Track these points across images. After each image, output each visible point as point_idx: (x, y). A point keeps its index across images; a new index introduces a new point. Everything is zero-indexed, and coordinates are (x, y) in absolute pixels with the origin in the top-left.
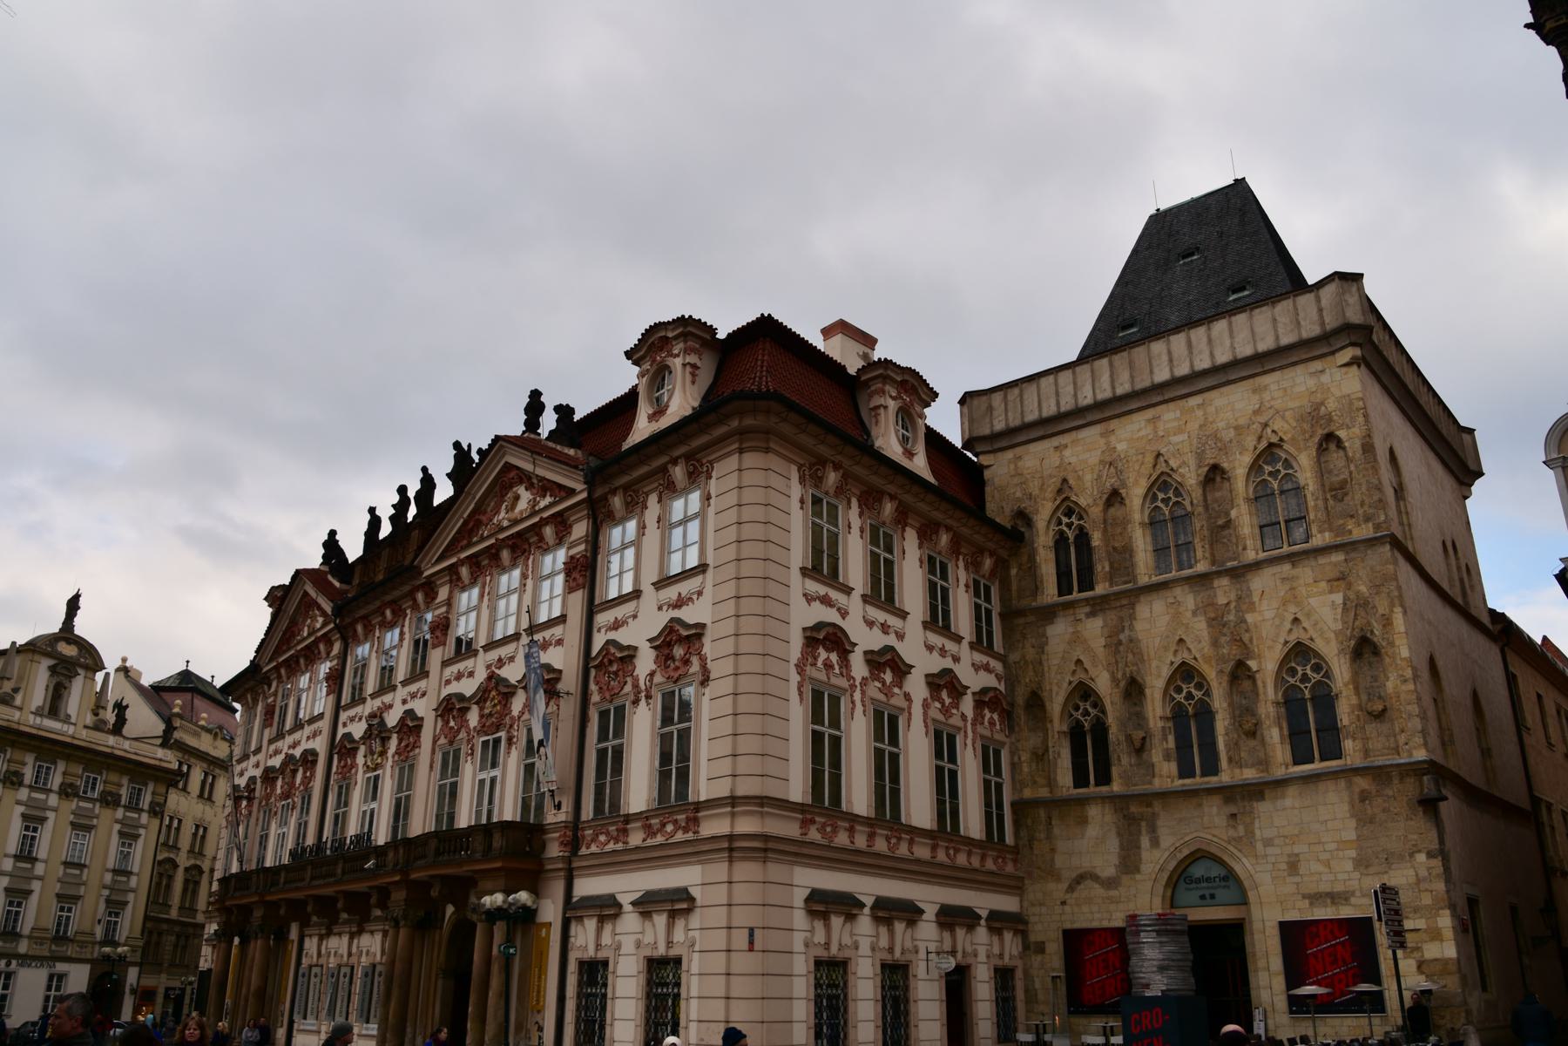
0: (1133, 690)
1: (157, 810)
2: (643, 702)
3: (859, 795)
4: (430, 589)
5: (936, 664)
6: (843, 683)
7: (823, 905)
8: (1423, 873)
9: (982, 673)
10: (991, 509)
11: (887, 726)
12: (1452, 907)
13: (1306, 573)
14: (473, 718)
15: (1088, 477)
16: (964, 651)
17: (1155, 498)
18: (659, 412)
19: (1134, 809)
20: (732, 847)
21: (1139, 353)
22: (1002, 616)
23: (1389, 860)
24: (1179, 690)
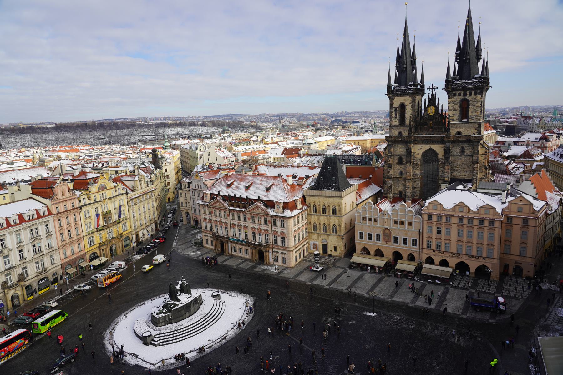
0: (320, 224)
7: (296, 252)
13: (335, 218)
23: (339, 242)
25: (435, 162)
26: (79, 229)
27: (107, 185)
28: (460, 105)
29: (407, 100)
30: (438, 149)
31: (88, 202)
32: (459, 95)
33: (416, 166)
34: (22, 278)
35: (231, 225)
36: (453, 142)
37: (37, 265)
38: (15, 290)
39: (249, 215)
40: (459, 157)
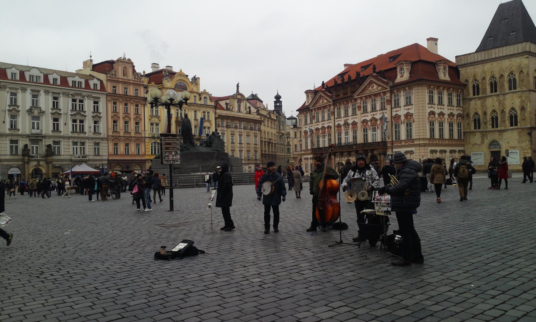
0: (485, 113)
1: (259, 130)
2: (403, 124)
3: (437, 136)
4: (356, 100)
5: (449, 112)
6: (434, 119)
7: (432, 152)
8: (527, 144)
9: (458, 111)
10: (461, 78)
11: (441, 124)
12: (532, 149)
13: (515, 95)
14: (369, 123)
15: (479, 74)
16: (455, 108)
17: (491, 79)
18: (402, 76)
19: (484, 133)
20: (419, 145)
22: (463, 99)
24: (493, 114)
26: (140, 124)
27: (189, 87)
34: (50, 151)
35: (336, 129)
37: (75, 147)
38: (38, 163)
39: (359, 101)
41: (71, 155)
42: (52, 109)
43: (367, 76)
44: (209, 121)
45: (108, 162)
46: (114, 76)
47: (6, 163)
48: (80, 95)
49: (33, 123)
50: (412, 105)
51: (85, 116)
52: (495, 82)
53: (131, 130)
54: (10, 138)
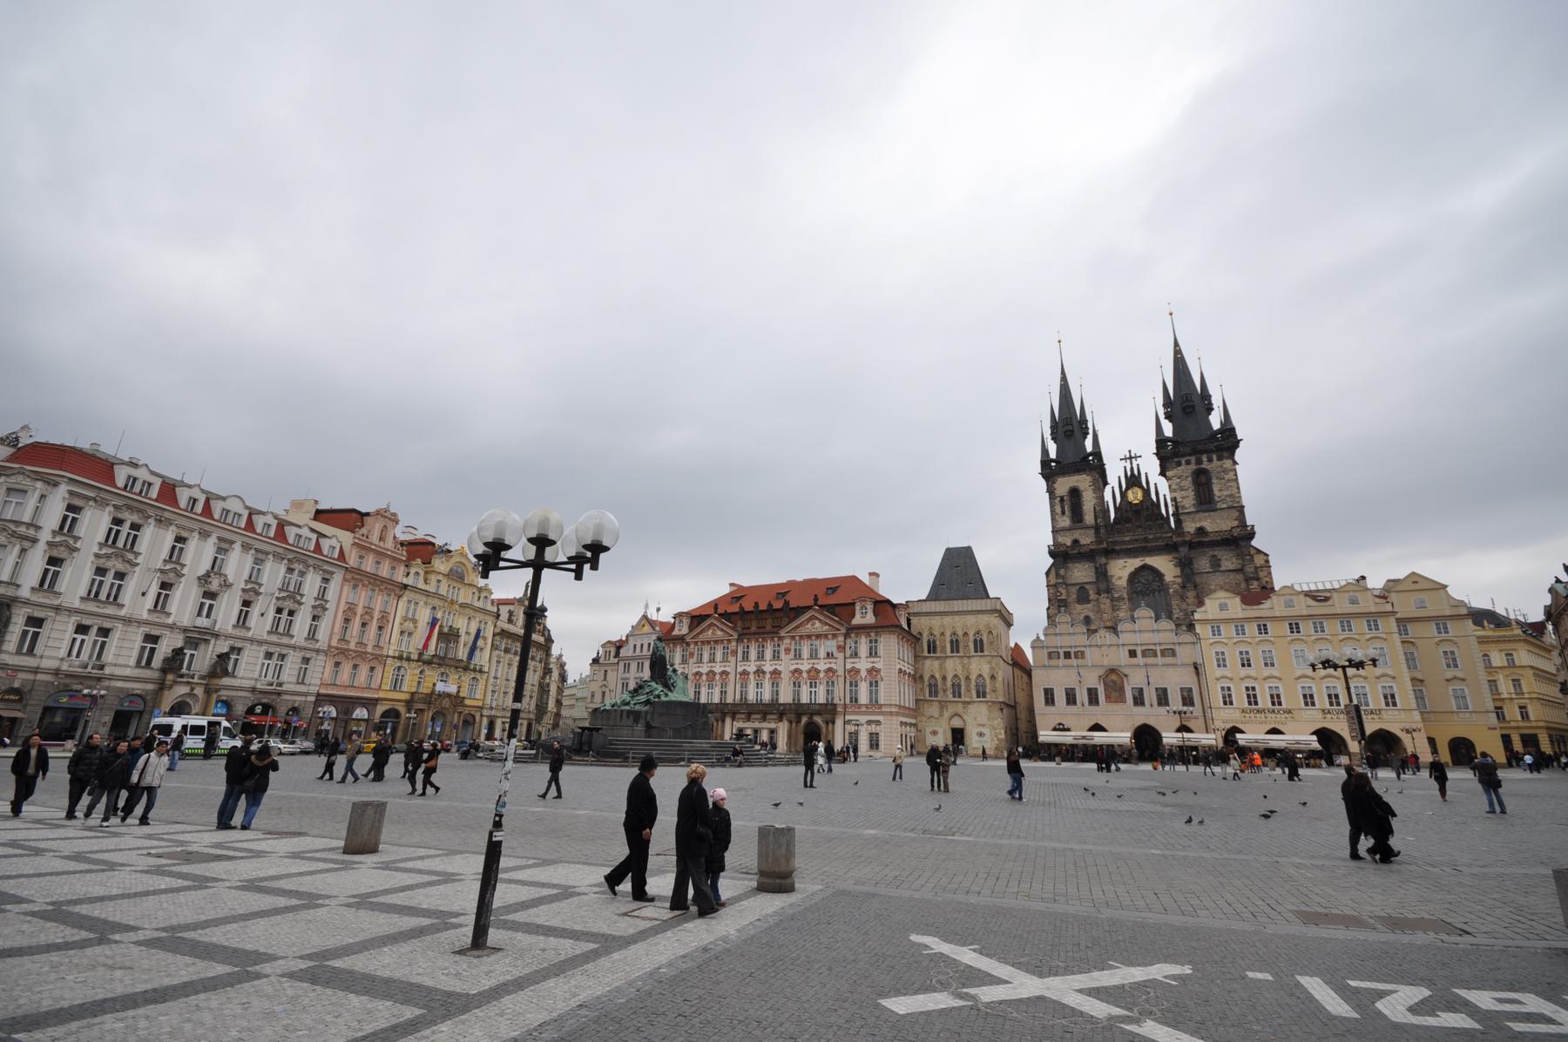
0: (944, 678)
4: (781, 638)
13: (982, 659)
14: (805, 675)
20: (891, 713)
21: (951, 602)
23: (994, 719)
25: (1159, 591)
26: (384, 630)
27: (468, 575)
28: (1193, 479)
29: (1083, 481)
30: (1165, 565)
31: (421, 585)
32: (1188, 463)
33: (1117, 603)
34: (222, 665)
36: (1192, 545)
37: (267, 662)
38: (192, 689)
39: (787, 641)
40: (1212, 577)
41: (256, 680)
42: (246, 581)
43: (809, 608)
44: (485, 639)
45: (316, 699)
46: (365, 538)
47: (119, 684)
48: (304, 562)
49: (202, 605)
50: (880, 657)
51: (300, 604)
52: (957, 640)
53: (368, 640)
54: (147, 629)
